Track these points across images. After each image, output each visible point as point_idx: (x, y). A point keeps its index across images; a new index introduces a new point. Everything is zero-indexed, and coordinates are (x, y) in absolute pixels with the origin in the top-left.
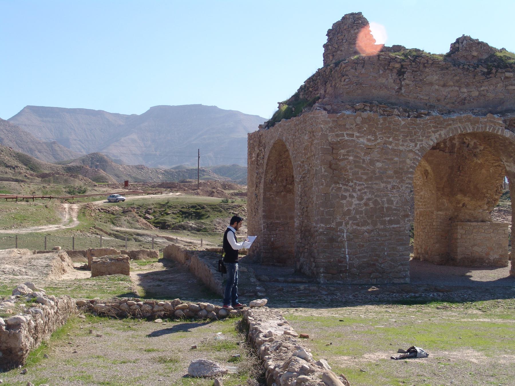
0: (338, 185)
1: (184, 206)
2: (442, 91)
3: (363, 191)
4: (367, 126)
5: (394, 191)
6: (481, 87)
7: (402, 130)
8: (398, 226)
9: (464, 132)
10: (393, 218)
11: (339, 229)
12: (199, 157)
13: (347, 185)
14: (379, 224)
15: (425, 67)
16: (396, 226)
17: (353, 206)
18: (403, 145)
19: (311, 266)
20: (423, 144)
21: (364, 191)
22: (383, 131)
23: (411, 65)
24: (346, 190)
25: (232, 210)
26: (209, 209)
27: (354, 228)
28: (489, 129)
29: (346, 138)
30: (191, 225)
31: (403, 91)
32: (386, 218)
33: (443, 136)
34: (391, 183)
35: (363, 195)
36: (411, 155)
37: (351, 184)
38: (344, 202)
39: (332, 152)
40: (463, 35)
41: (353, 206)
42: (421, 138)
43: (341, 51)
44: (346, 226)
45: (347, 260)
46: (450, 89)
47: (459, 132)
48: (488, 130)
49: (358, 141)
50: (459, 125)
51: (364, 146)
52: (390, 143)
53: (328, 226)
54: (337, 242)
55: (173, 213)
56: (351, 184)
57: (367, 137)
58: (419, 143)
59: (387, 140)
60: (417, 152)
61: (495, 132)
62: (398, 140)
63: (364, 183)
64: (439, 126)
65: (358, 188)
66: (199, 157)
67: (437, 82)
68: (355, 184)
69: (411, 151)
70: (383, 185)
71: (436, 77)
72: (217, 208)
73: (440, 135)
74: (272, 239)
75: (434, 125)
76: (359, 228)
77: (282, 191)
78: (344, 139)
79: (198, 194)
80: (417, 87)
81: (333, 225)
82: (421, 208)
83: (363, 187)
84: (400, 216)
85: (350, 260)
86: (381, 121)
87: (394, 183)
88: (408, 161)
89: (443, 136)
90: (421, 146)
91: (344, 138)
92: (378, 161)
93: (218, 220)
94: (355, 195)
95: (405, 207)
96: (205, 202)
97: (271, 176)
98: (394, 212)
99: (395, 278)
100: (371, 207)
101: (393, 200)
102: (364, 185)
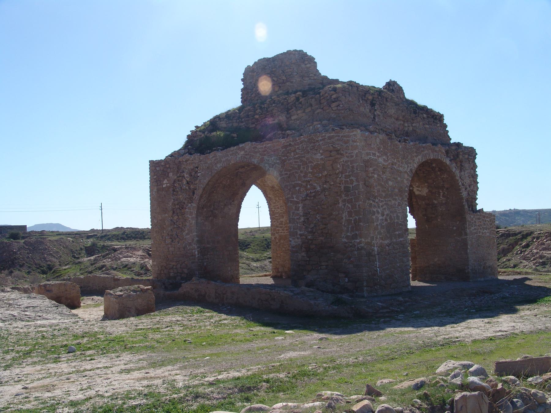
3: (384, 207)
5: (399, 207)
14: (393, 238)
17: (379, 221)
19: (339, 282)
23: (378, 98)
24: (375, 207)
31: (377, 120)
40: (391, 80)
41: (379, 221)
43: (292, 82)
52: (396, 163)
53: (366, 241)
54: (372, 256)
56: (377, 200)
58: (409, 165)
65: (381, 204)
70: (393, 202)
74: (205, 263)
76: (383, 242)
77: (210, 216)
81: (369, 240)
82: (281, 233)
84: (403, 231)
85: (380, 273)
86: (390, 144)
97: (204, 201)
98: (400, 227)
99: (403, 287)
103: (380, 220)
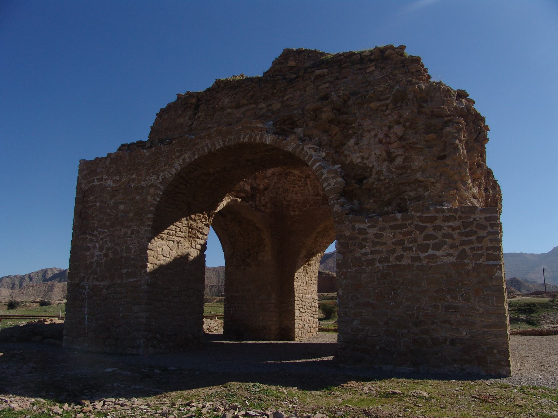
0: (84, 236)
1: (521, 305)
2: (235, 114)
4: (114, 166)
5: (134, 236)
6: (284, 96)
7: (145, 163)
8: (135, 279)
9: (212, 149)
10: (130, 270)
11: (81, 285)
12: (544, 272)
13: (92, 235)
15: (217, 92)
16: (132, 280)
17: (95, 258)
18: (145, 180)
20: (165, 174)
21: (106, 239)
22: (128, 168)
24: (91, 240)
25: (556, 306)
26: (539, 307)
27: (94, 283)
28: (244, 138)
29: (96, 183)
30: (522, 318)
32: (123, 271)
33: (188, 160)
34: (131, 227)
35: (104, 244)
36: (152, 190)
37: (96, 233)
38: (88, 253)
39: (83, 201)
41: (95, 258)
42: (164, 168)
44: (88, 281)
45: (86, 322)
46: (246, 108)
47: (206, 150)
48: (242, 140)
49: (105, 184)
50: (208, 142)
51: (110, 189)
52: (133, 180)
55: (513, 310)
56: (96, 233)
57: (114, 178)
58: (161, 174)
59: (131, 177)
60: (159, 185)
61: (252, 140)
62: (141, 175)
63: (107, 231)
64: (184, 149)
66: (544, 272)
67: (229, 104)
68: (100, 233)
69: (152, 186)
70: (123, 230)
71: (227, 100)
72: (544, 306)
73: (184, 160)
74: (232, 312)
75: (179, 148)
76: (98, 284)
78: (93, 185)
79: (543, 297)
80: (208, 117)
83: (105, 234)
87: (135, 227)
88: (149, 198)
89: (188, 160)
90: (164, 177)
91: (94, 183)
92: (121, 203)
93: (543, 314)
94: (97, 245)
95: (142, 255)
96: (537, 302)
97: (229, 251)
98: (132, 262)
100: (110, 258)
101: (131, 248)
102: (106, 233)
103: (97, 256)
